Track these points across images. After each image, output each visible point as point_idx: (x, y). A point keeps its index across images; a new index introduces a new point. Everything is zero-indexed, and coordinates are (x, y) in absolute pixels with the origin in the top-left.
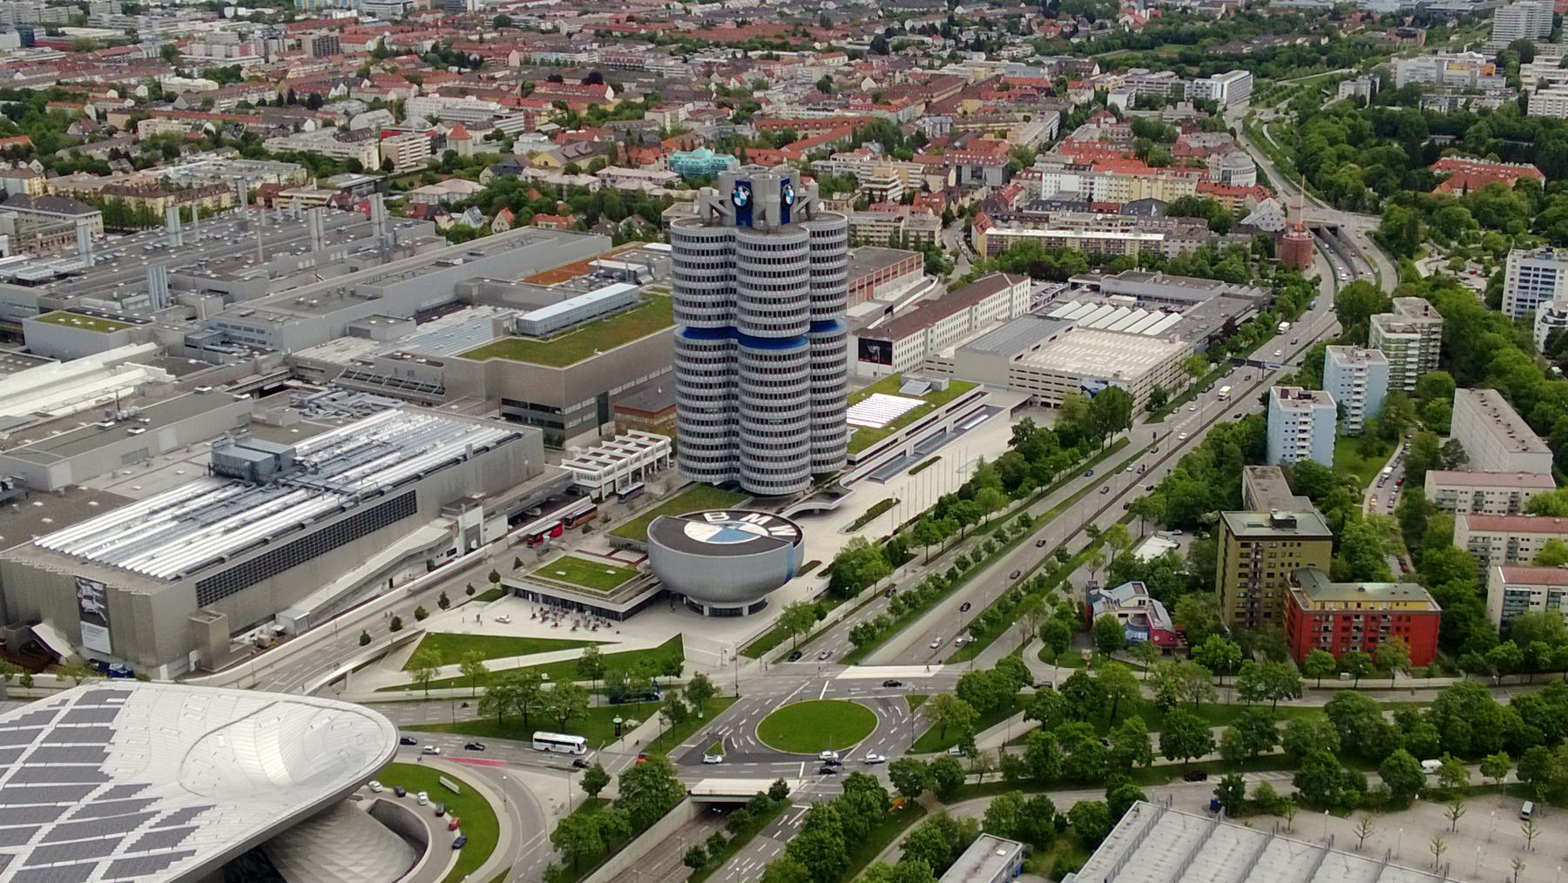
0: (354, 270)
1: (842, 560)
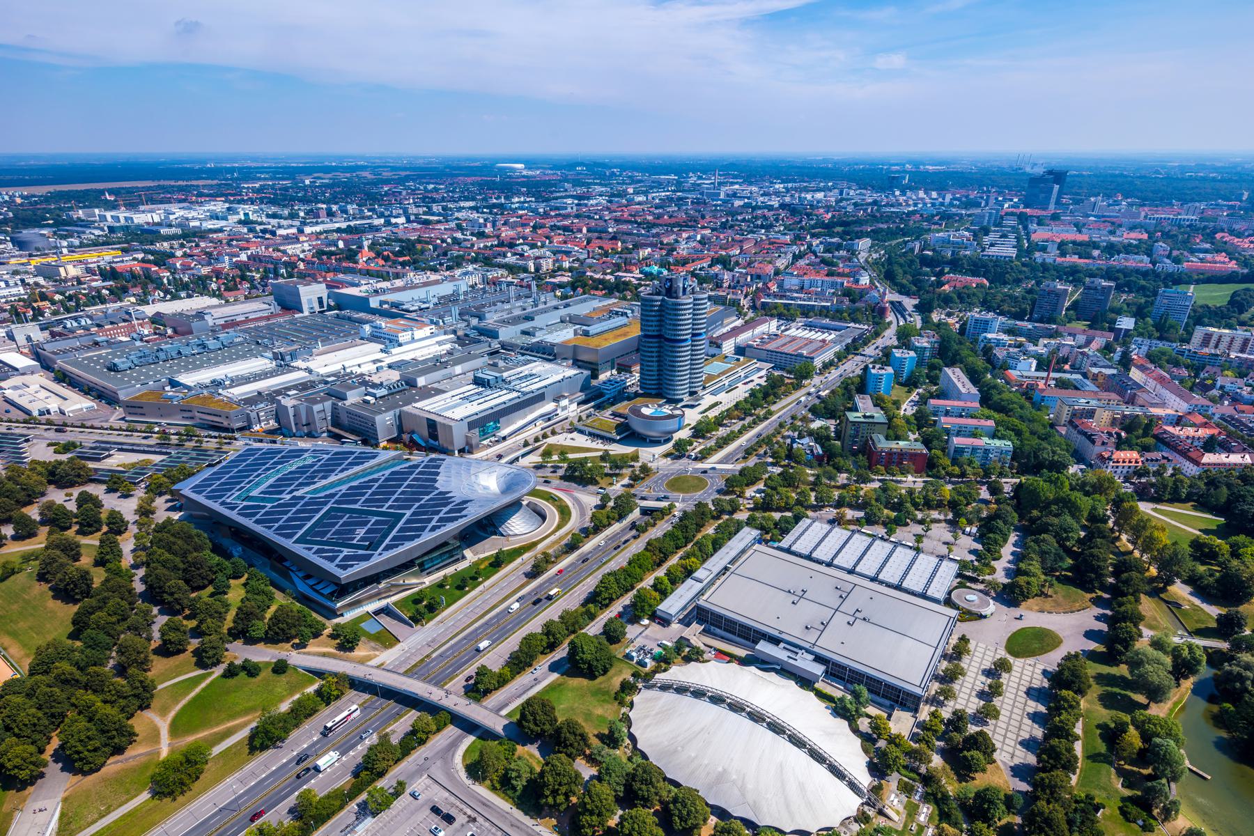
0: (524, 309)
1: (699, 423)
